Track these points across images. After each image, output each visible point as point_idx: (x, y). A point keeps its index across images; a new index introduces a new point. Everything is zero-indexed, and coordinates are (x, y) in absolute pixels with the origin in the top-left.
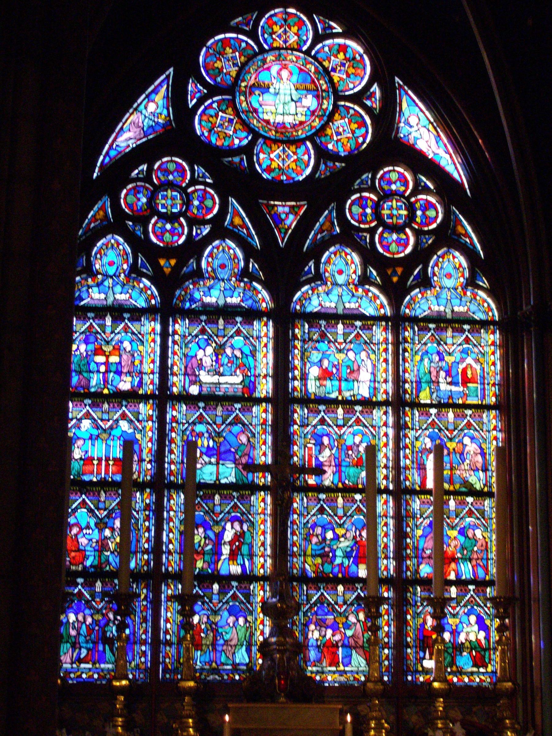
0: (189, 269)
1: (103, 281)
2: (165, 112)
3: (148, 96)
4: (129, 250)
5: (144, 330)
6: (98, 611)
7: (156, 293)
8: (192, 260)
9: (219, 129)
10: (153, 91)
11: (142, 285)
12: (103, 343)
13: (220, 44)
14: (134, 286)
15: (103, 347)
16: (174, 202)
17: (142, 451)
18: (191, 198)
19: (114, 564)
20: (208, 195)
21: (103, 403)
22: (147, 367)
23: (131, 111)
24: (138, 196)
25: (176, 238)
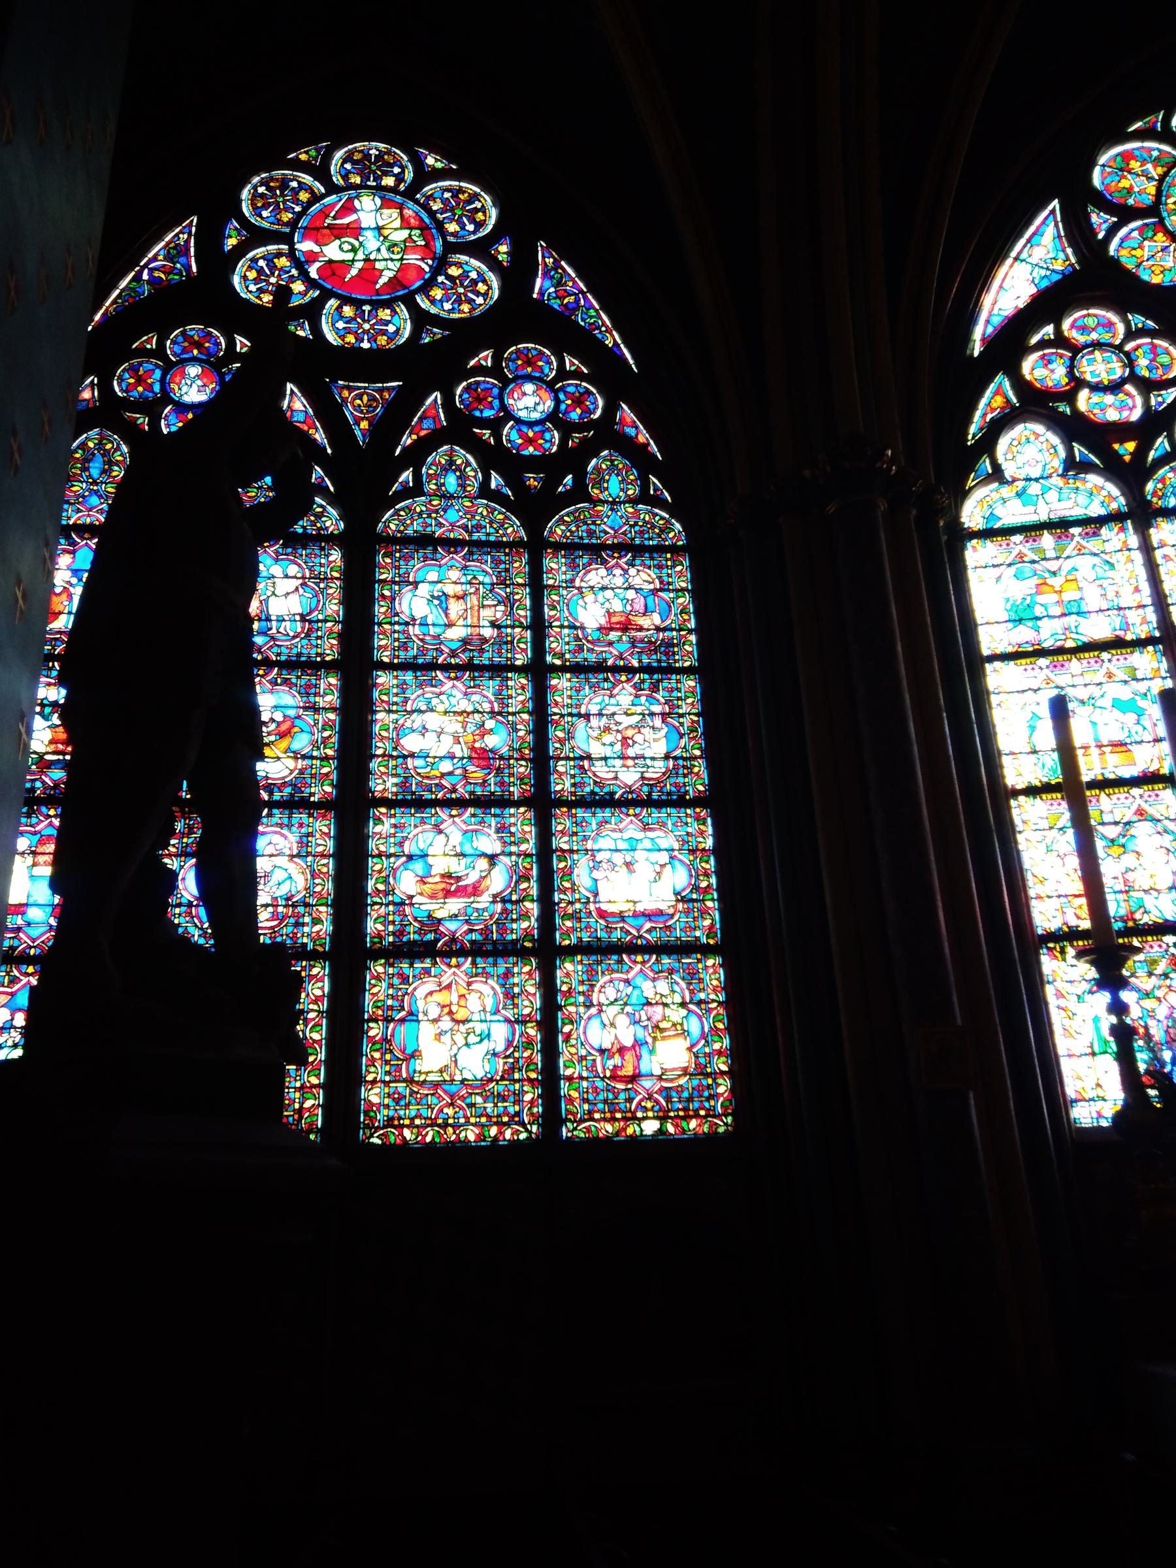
0: (1159, 453)
1: (1024, 490)
2: (1061, 256)
3: (1029, 241)
4: (1055, 440)
5: (1108, 547)
6: (1147, 995)
7: (1115, 491)
8: (1160, 440)
9: (1150, 263)
10: (1034, 234)
11: (1089, 485)
12: (1047, 575)
13: (1119, 159)
14: (1077, 489)
15: (1048, 581)
16: (1109, 366)
17: (1155, 725)
18: (1134, 358)
19: (1155, 912)
20: (1159, 350)
21: (1070, 660)
22: (1128, 599)
23: (1009, 261)
24: (1050, 366)
25: (1125, 414)
